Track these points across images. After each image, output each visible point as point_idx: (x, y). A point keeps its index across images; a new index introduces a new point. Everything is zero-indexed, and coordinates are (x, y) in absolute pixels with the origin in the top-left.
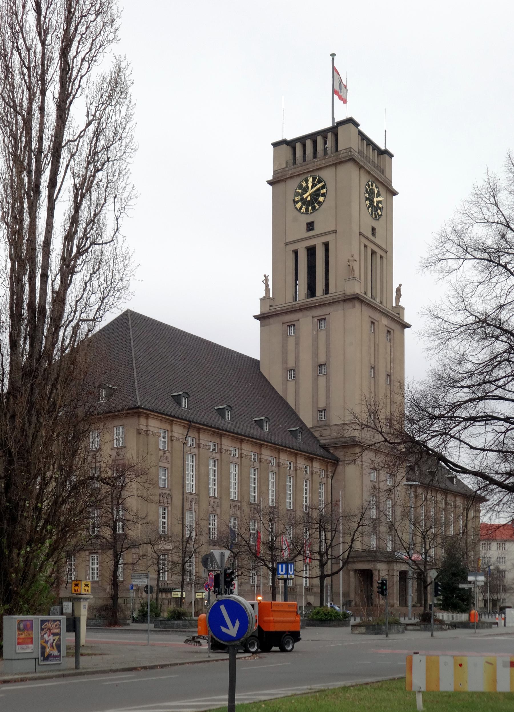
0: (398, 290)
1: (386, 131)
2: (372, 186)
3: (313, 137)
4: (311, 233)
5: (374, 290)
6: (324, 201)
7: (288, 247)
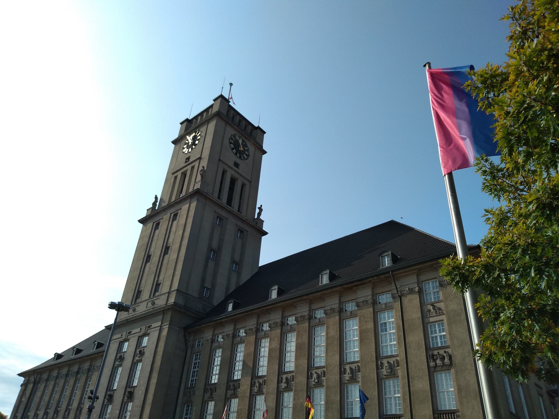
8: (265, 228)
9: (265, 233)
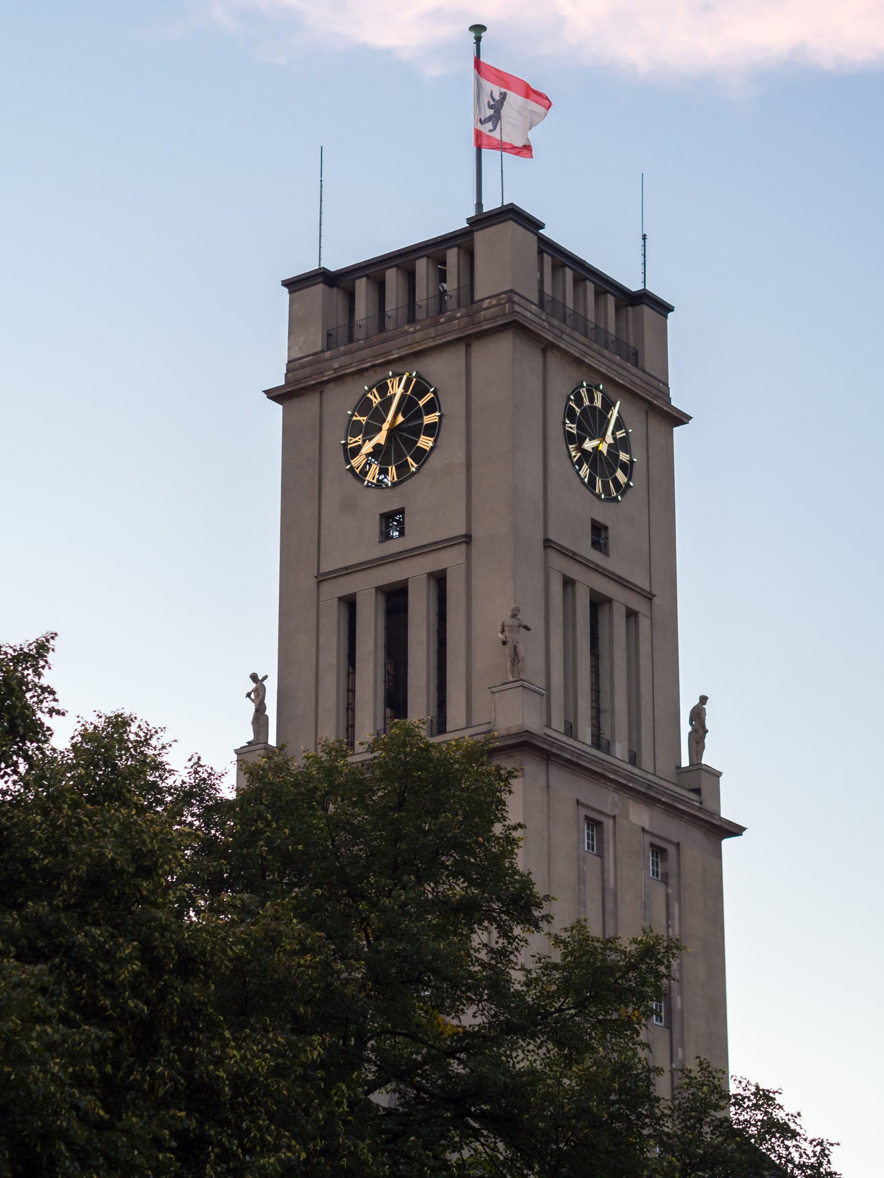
0: (698, 715)
1: (644, 237)
2: (592, 399)
3: (404, 260)
5: (605, 719)
6: (432, 449)
7: (325, 586)
8: (729, 810)
9: (736, 830)
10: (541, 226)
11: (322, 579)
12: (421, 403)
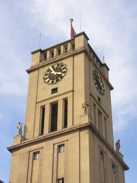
1: (104, 57)
4: (55, 94)
10: (88, 39)
11: (37, 103)
12: (62, 68)
